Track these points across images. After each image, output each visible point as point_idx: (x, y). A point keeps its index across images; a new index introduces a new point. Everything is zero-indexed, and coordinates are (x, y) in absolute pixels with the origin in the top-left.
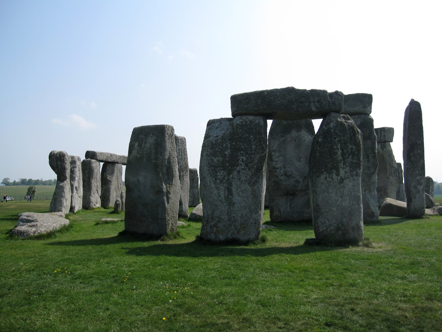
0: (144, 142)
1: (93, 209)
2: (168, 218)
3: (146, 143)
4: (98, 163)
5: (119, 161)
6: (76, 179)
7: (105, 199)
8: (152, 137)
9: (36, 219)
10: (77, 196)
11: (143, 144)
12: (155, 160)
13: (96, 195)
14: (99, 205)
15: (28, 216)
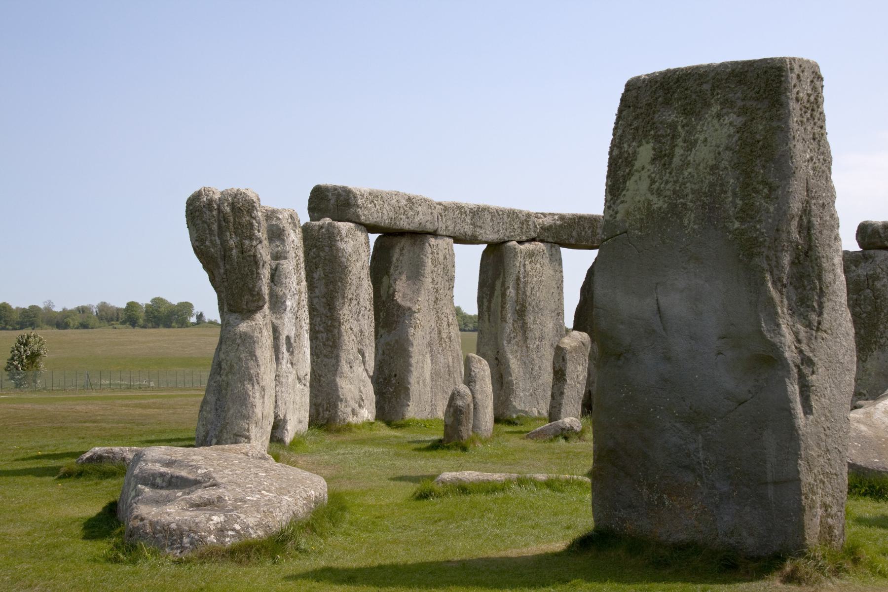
0: (680, 142)
1: (349, 427)
2: (807, 478)
3: (691, 145)
4: (361, 236)
5: (441, 226)
6: (288, 303)
7: (390, 386)
8: (719, 116)
9: (208, 476)
10: (292, 378)
11: (679, 151)
12: (742, 220)
13: (359, 369)
14: (367, 413)
15: (169, 464)
